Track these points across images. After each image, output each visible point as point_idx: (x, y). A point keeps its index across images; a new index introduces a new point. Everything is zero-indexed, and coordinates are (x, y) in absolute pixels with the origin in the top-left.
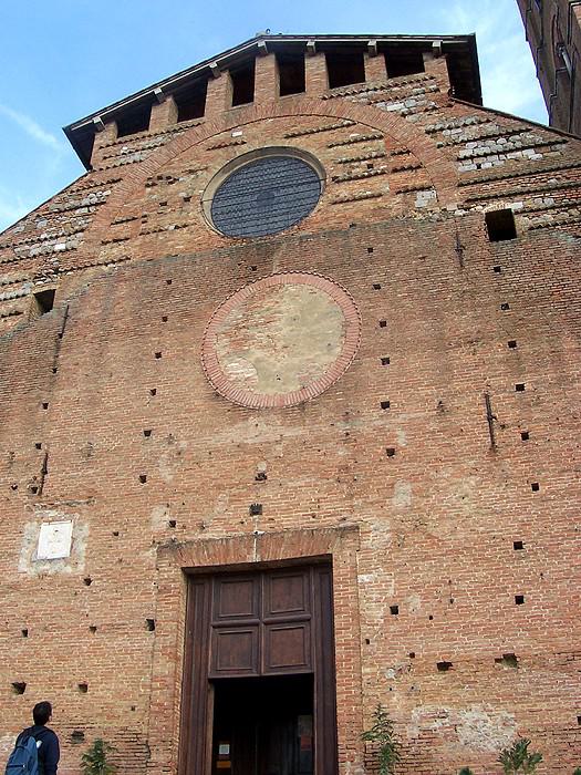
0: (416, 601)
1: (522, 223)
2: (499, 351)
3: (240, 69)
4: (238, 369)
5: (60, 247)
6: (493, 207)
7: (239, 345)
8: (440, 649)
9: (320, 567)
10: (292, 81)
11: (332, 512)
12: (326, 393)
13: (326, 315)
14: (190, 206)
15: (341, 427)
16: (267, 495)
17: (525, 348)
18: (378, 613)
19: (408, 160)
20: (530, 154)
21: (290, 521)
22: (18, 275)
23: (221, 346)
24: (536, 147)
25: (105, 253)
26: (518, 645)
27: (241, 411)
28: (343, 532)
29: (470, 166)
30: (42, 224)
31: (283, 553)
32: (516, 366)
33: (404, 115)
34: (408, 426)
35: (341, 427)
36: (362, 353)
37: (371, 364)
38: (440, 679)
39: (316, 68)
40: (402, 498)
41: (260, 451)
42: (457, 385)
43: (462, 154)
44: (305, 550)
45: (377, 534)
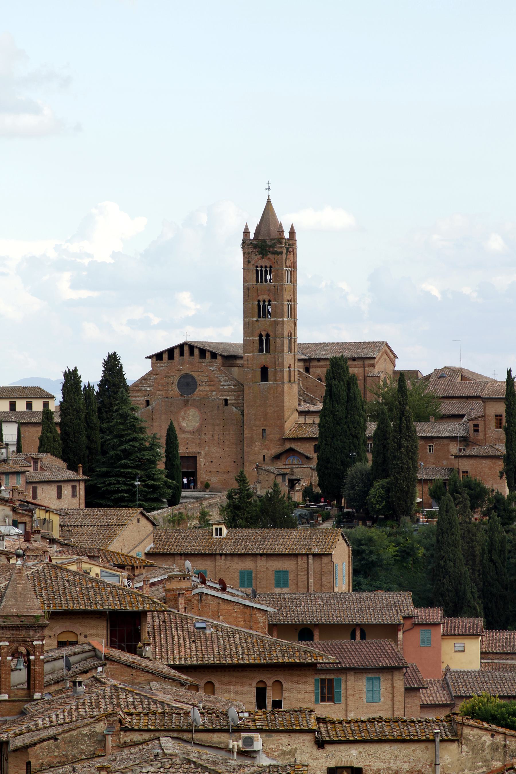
0: (207, 464)
1: (229, 402)
2: (222, 428)
3: (181, 347)
4: (183, 424)
5: (148, 389)
7: (184, 420)
8: (210, 470)
9: (196, 457)
10: (192, 353)
11: (197, 450)
12: (197, 430)
13: (197, 416)
14: (173, 385)
15: (199, 437)
16: (188, 446)
17: (225, 427)
18: (203, 465)
19: (212, 383)
20: (233, 387)
21: (191, 451)
22: (140, 395)
23: (181, 419)
24: (234, 386)
25: (158, 393)
26: (219, 470)
27: (184, 432)
28: (199, 453)
29: (222, 387)
30: (143, 382)
31: (190, 455)
32: (223, 430)
33: (212, 371)
34: (208, 438)
35: (199, 437)
37: (204, 426)
38: (209, 473)
39: (196, 351)
40: (206, 449)
41: (187, 439)
42: (215, 432)
43: (222, 384)
44: (193, 455)
45: (203, 453)
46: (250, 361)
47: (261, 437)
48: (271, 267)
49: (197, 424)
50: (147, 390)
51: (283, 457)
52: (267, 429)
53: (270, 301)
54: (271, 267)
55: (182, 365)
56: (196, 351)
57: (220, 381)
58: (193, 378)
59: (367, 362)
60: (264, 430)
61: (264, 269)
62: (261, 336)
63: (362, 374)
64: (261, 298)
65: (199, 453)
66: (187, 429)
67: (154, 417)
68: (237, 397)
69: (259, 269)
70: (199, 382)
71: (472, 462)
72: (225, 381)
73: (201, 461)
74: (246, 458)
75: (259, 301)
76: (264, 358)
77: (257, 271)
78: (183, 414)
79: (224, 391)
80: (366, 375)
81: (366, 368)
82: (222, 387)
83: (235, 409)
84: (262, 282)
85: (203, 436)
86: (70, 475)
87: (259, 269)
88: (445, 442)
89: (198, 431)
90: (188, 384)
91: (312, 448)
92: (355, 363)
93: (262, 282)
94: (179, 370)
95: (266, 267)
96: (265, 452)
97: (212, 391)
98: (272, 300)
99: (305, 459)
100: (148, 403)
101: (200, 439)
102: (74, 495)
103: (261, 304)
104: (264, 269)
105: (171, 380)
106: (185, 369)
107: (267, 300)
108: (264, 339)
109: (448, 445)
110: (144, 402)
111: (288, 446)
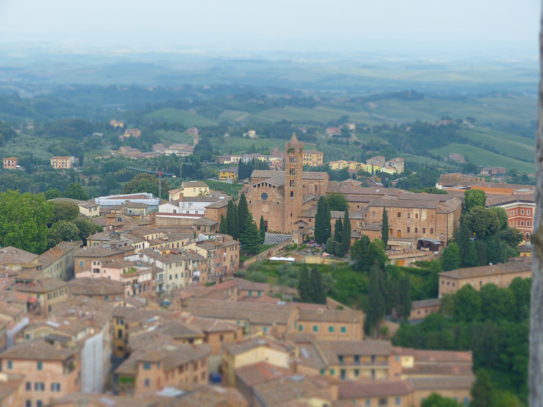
1: (279, 203)
4: (263, 210)
6: (277, 201)
7: (263, 208)
9: (267, 221)
11: (268, 219)
18: (269, 224)
20: (281, 198)
23: (262, 208)
27: (263, 212)
36: (269, 210)
39: (268, 185)
40: (271, 219)
45: (270, 220)
46: (287, 190)
47: (290, 216)
48: (295, 157)
49: (268, 210)
50: (250, 198)
51: (298, 223)
52: (292, 213)
53: (294, 169)
54: (295, 157)
55: (263, 189)
56: (268, 185)
57: (276, 196)
58: (266, 194)
59: (321, 181)
60: (291, 214)
61: (292, 158)
62: (291, 181)
63: (319, 184)
64: (291, 168)
65: (268, 220)
66: (264, 211)
67: (253, 207)
68: (282, 201)
69: (291, 158)
70: (268, 196)
71: (367, 232)
72: (278, 196)
73: (269, 223)
74: (285, 223)
75: (290, 169)
76: (292, 189)
77: (290, 159)
78: (263, 206)
79: (277, 199)
80: (320, 185)
81: (320, 183)
82: (277, 198)
83: (281, 205)
84: (292, 162)
85: (270, 214)
86: (234, 242)
87: (291, 158)
88: (355, 220)
89: (268, 213)
90: (264, 196)
91: (308, 220)
92: (317, 181)
93: (292, 162)
94: (262, 191)
95: (293, 157)
96: (292, 221)
97: (273, 199)
98: (295, 169)
99: (306, 224)
100: (250, 202)
101: (269, 215)
102: (236, 249)
103: (291, 170)
104: (292, 158)
105: (259, 194)
106: (264, 191)
107: (293, 169)
108: (292, 182)
109: (356, 221)
110: (249, 202)
111: (300, 219)
